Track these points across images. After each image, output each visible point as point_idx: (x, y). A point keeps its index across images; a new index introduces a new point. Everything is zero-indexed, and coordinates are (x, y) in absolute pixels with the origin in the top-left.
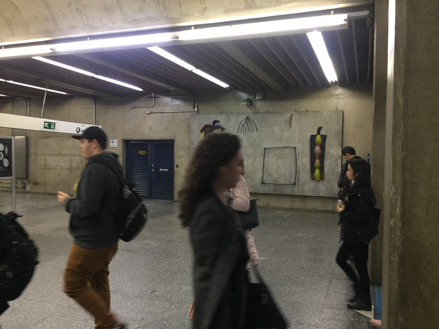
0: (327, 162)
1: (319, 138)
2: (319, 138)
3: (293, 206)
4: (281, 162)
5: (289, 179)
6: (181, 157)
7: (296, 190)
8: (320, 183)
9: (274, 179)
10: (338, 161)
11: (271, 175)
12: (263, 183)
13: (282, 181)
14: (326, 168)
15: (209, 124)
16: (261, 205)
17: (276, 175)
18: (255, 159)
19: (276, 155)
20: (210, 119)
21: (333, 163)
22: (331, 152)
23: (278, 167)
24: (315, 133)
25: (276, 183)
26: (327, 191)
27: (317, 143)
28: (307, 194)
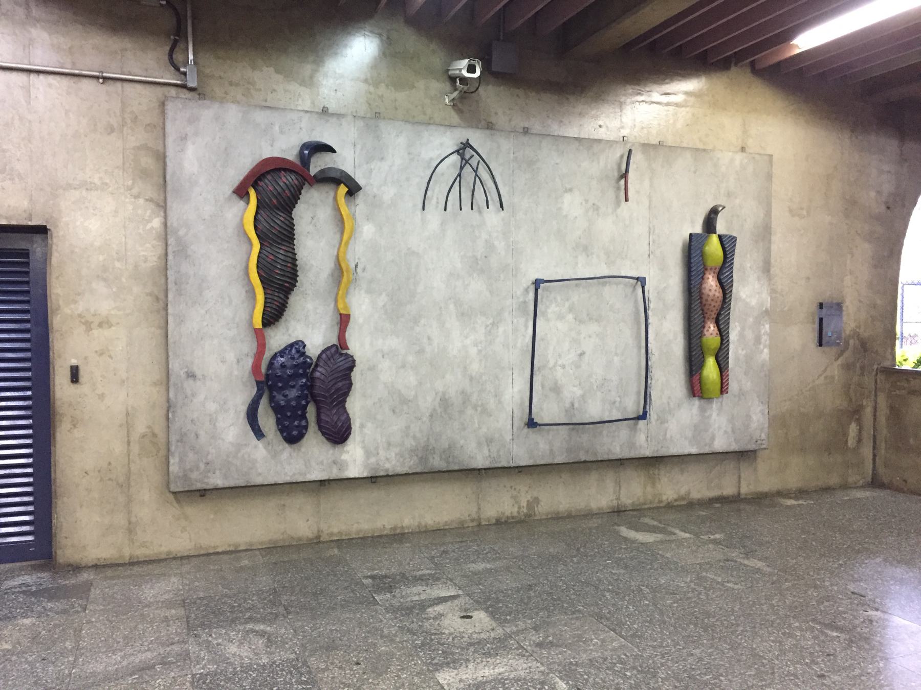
1: (714, 246)
2: (714, 246)
3: (618, 499)
4: (590, 337)
5: (618, 399)
6: (100, 325)
7: (641, 438)
8: (714, 406)
9: (567, 405)
10: (762, 327)
11: (556, 389)
12: (531, 423)
13: (595, 410)
15: (276, 155)
16: (509, 515)
17: (574, 386)
18: (493, 324)
19: (571, 310)
20: (282, 132)
21: (749, 335)
23: (582, 354)
24: (698, 229)
25: (575, 421)
26: (733, 431)
27: (710, 263)
28: (674, 451)
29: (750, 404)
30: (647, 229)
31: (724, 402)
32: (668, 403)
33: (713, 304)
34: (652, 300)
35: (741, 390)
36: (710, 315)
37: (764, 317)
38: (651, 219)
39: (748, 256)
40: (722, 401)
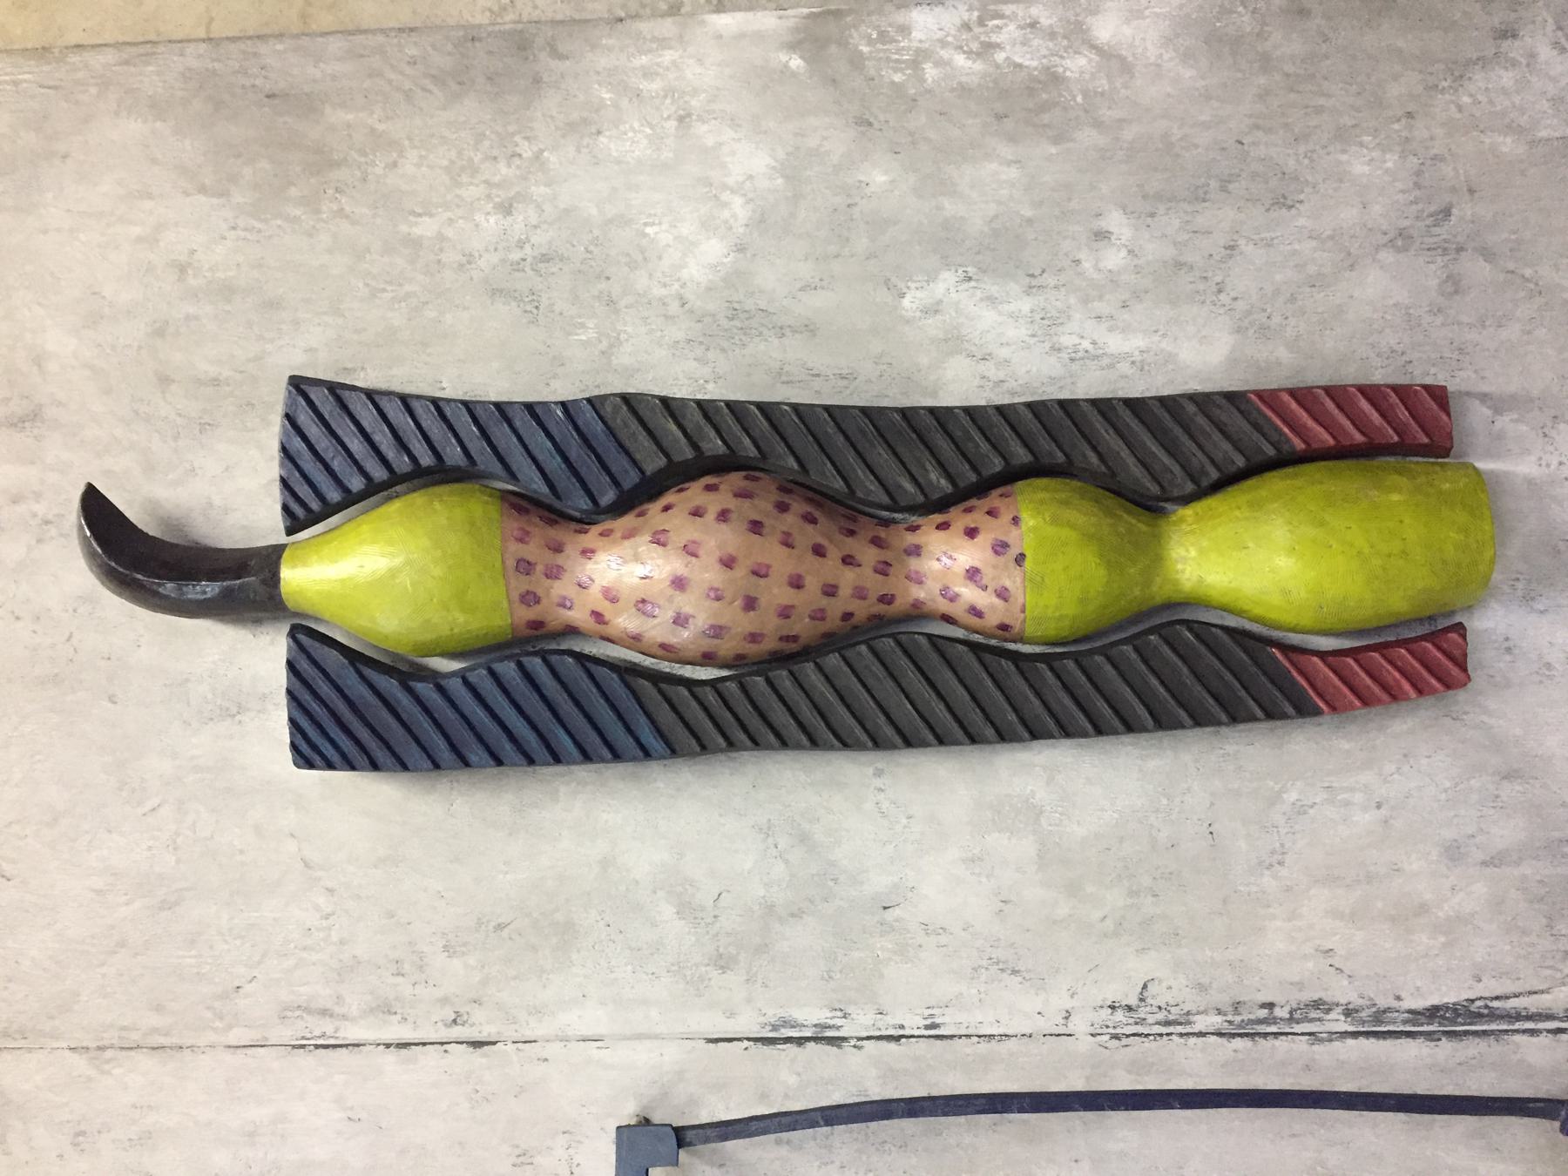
0: (954, 342)
10: (930, 72)
14: (1116, 343)
22: (714, 250)
29: (1508, 145)
30: (306, 1060)
31: (1511, 383)
32: (1494, 861)
33: (775, 593)
34: (773, 1014)
35: (1401, 240)
36: (860, 593)
37: (857, 61)
38: (235, 1036)
39: (426, 228)
40: (1484, 397)
